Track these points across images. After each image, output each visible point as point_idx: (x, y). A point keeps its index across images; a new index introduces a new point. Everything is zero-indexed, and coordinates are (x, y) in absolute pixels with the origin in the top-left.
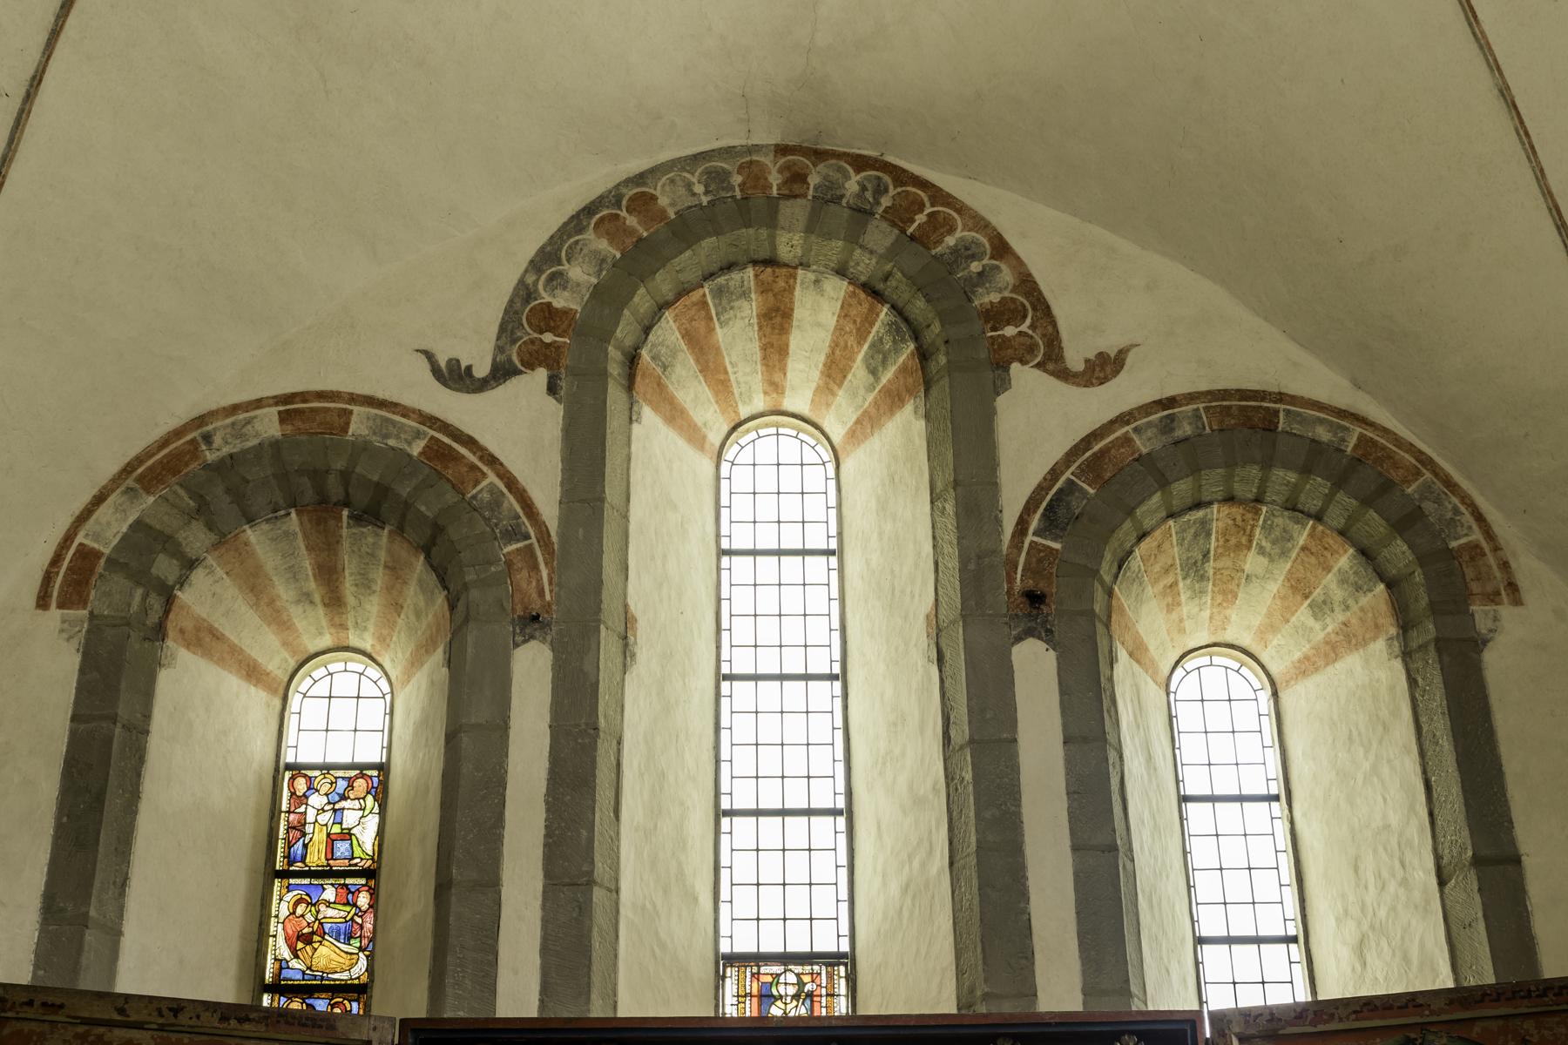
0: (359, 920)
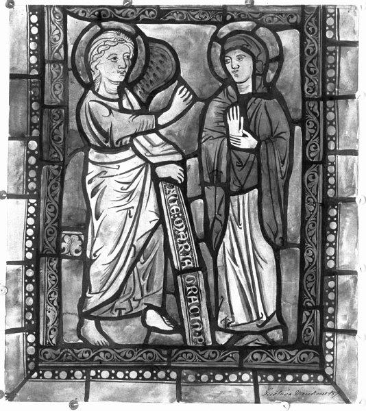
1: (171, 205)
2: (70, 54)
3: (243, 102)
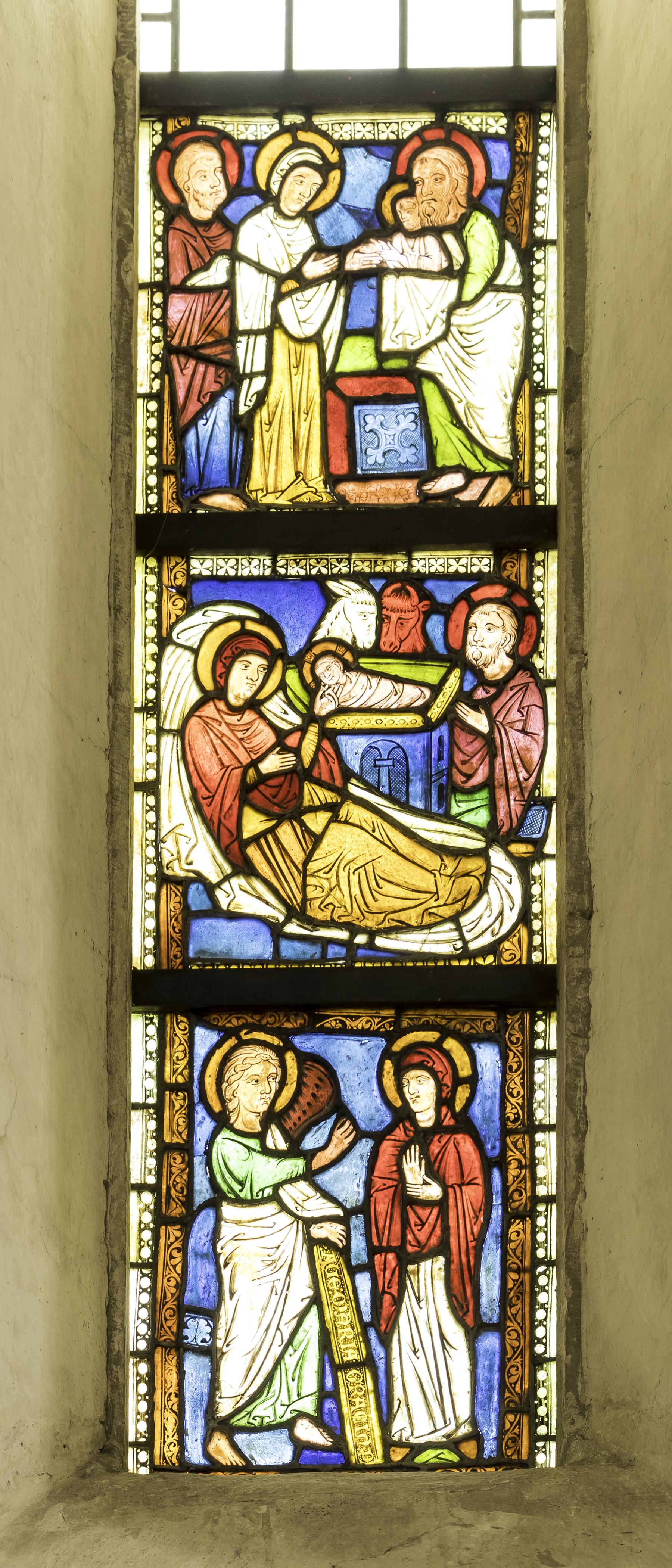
0: (478, 721)
1: (329, 1275)
2: (196, 1074)
3: (423, 1137)
